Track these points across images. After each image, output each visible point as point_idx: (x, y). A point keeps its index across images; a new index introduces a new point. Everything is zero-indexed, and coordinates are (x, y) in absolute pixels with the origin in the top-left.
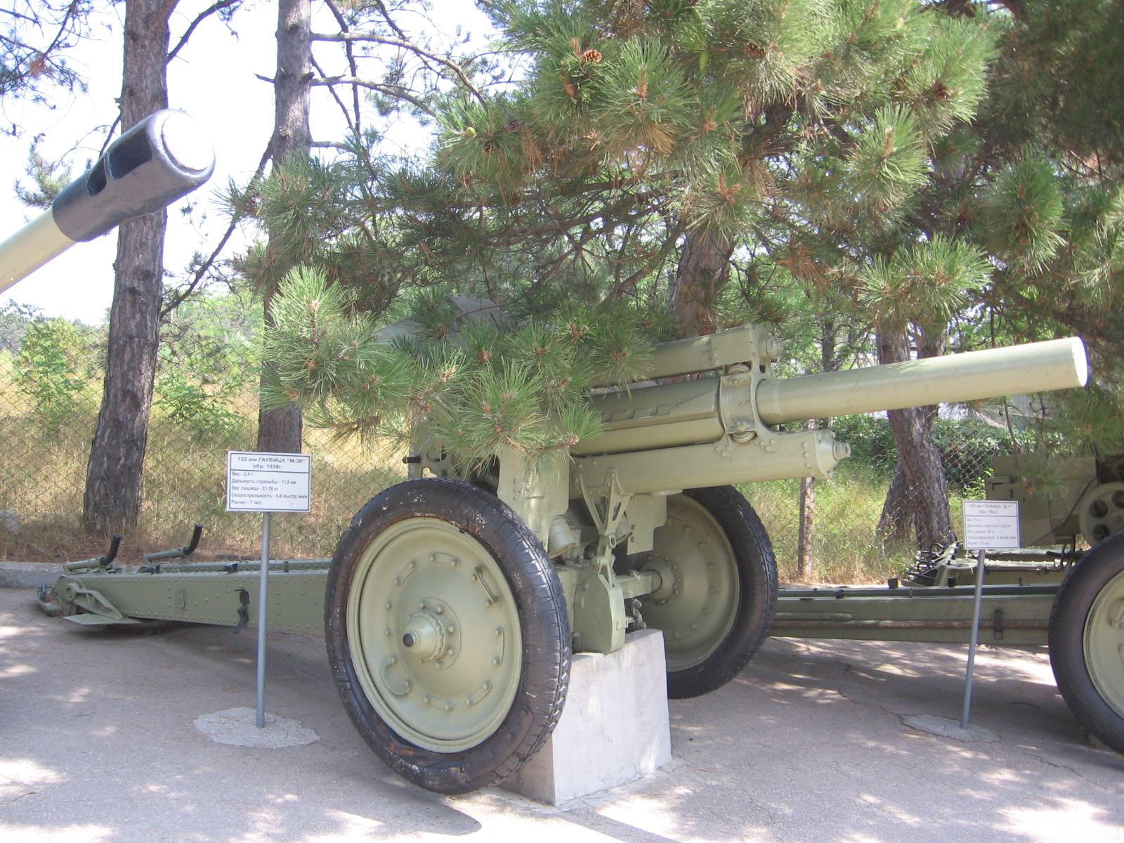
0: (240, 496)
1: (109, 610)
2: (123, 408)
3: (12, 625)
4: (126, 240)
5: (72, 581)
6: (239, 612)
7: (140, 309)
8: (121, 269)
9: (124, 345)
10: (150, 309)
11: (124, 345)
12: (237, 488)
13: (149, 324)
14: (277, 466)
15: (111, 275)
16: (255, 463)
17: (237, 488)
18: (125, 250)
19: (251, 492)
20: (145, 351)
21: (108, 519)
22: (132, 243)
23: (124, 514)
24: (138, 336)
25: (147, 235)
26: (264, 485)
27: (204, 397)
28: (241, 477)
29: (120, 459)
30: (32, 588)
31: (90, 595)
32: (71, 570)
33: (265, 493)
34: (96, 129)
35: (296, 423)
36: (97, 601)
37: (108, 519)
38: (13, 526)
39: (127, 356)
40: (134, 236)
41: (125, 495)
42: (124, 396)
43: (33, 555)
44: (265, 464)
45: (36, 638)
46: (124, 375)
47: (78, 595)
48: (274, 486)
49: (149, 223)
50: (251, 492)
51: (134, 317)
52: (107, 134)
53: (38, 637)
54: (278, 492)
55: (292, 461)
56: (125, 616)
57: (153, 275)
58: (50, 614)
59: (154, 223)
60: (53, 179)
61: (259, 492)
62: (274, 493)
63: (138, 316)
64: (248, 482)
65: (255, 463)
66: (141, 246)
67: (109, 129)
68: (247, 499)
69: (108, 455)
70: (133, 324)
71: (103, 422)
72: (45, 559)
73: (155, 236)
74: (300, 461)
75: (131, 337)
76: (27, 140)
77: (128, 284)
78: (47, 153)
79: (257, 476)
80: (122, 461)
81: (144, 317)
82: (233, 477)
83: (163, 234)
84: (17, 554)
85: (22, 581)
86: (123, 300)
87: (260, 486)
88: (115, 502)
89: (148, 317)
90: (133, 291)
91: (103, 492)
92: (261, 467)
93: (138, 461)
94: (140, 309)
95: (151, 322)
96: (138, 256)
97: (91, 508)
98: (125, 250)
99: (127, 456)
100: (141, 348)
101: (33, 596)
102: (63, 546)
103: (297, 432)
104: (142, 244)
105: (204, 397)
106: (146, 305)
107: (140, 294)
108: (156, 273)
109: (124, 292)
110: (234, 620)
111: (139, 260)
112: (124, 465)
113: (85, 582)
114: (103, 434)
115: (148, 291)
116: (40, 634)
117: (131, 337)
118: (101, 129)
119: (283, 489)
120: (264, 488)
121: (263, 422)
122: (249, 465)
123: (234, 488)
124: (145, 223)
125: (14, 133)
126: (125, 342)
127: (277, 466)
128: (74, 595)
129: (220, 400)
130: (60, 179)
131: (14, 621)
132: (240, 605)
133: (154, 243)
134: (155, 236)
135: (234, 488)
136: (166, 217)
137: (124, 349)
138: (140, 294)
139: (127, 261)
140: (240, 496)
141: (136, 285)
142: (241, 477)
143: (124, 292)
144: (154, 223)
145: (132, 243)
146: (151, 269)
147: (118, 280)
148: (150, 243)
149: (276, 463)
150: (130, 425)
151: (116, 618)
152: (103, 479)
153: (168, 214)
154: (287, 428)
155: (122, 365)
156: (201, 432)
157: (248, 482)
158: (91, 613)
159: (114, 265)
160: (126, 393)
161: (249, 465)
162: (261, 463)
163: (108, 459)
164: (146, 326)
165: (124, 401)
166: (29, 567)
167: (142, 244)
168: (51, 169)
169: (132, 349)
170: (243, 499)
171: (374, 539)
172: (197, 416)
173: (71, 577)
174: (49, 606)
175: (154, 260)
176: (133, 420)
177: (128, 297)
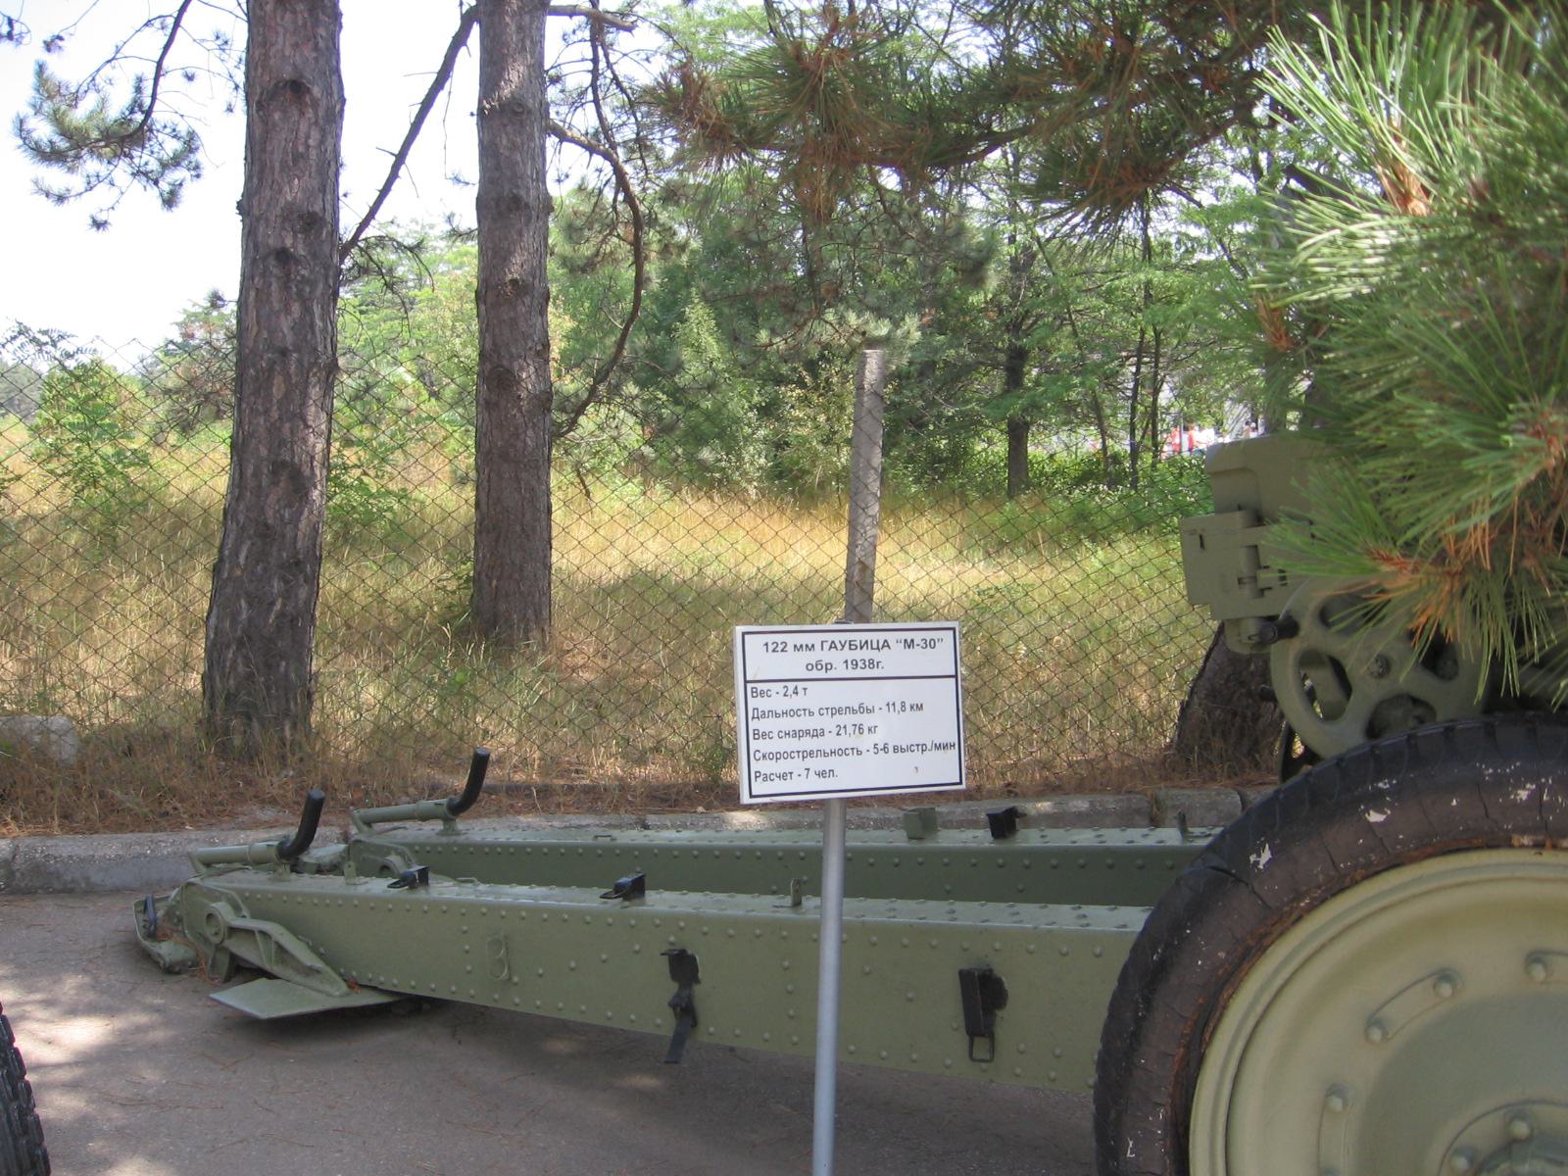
0: (777, 756)
1: (310, 971)
2: (272, 499)
3: (91, 1010)
4: (263, 150)
5: (215, 896)
6: (673, 1005)
7: (300, 293)
8: (255, 211)
9: (271, 370)
10: (319, 292)
11: (271, 370)
13: (319, 323)
14: (872, 664)
15: (235, 225)
16: (812, 657)
18: (262, 171)
19: (808, 744)
20: (314, 380)
21: (255, 724)
22: (277, 157)
23: (287, 713)
24: (298, 349)
25: (308, 137)
26: (840, 719)
27: (346, 468)
28: (776, 701)
29: (273, 603)
30: (116, 891)
31: (263, 933)
32: (208, 865)
33: (845, 741)
34: (148, 24)
35: (542, 506)
36: (281, 949)
37: (255, 724)
38: (67, 750)
39: (278, 390)
40: (279, 142)
41: (286, 675)
42: (274, 473)
43: (114, 818)
44: (836, 658)
45: (152, 1051)
46: (273, 429)
47: (233, 931)
48: (866, 720)
49: (310, 113)
50: (808, 744)
51: (287, 310)
52: (169, 31)
53: (155, 1046)
54: (879, 738)
55: (909, 644)
56: (354, 985)
57: (322, 219)
58: (170, 970)
59: (321, 113)
60: (79, 115)
61: (828, 742)
62: (866, 742)
63: (296, 308)
65: (812, 657)
66: (295, 161)
67: (170, 22)
68: (796, 765)
69: (248, 595)
70: (285, 324)
71: (232, 526)
72: (140, 823)
73: (322, 142)
74: (930, 644)
75: (284, 353)
76: (32, 51)
77: (271, 241)
78: (67, 69)
79: (819, 695)
80: (278, 606)
81: (307, 310)
83: (338, 137)
84: (80, 816)
85: (96, 878)
86: (263, 275)
87: (828, 723)
88: (268, 689)
89: (317, 310)
90: (283, 256)
91: (241, 668)
92: (828, 667)
93: (307, 602)
94: (300, 293)
95: (323, 320)
96: (290, 182)
97: (220, 703)
98: (262, 171)
99: (288, 594)
100: (305, 373)
101: (120, 918)
102: (173, 791)
103: (544, 523)
104: (298, 158)
105: (346, 468)
106: (313, 284)
107: (298, 262)
108: (328, 219)
109: (264, 259)
110: (663, 1023)
111: (293, 191)
112: (282, 615)
113: (245, 899)
114: (236, 553)
115: (314, 256)
116: (159, 1035)
117: (284, 353)
118: (157, 24)
119: (889, 727)
120: (840, 730)
121: (484, 506)
122: (793, 664)
123: (756, 732)
124: (302, 114)
125: (10, 36)
126: (272, 363)
127: (872, 664)
128: (223, 930)
129: (372, 473)
130: (90, 118)
131: (91, 996)
132: (673, 987)
133: (322, 153)
134: (322, 142)
136: (343, 101)
137: (270, 379)
138: (298, 262)
139: (268, 193)
140: (777, 756)
141: (289, 242)
142: (776, 701)
143: (264, 259)
144: (321, 113)
145: (277, 157)
146: (317, 208)
147: (250, 235)
148: (313, 153)
149: (866, 654)
150: (289, 531)
151: (332, 995)
152: (240, 643)
153: (347, 94)
154: (528, 516)
155: (266, 412)
156: (347, 526)
158: (270, 976)
159: (240, 206)
160: (278, 467)
161: (793, 664)
162: (828, 656)
163: (250, 605)
164: (312, 325)
165: (276, 483)
166: (109, 846)
167: (298, 158)
168: (75, 99)
169: (287, 377)
171: (1312, 908)
172: (337, 500)
173: (211, 883)
174: (167, 950)
175: (323, 190)
176: (295, 520)
177: (275, 269)
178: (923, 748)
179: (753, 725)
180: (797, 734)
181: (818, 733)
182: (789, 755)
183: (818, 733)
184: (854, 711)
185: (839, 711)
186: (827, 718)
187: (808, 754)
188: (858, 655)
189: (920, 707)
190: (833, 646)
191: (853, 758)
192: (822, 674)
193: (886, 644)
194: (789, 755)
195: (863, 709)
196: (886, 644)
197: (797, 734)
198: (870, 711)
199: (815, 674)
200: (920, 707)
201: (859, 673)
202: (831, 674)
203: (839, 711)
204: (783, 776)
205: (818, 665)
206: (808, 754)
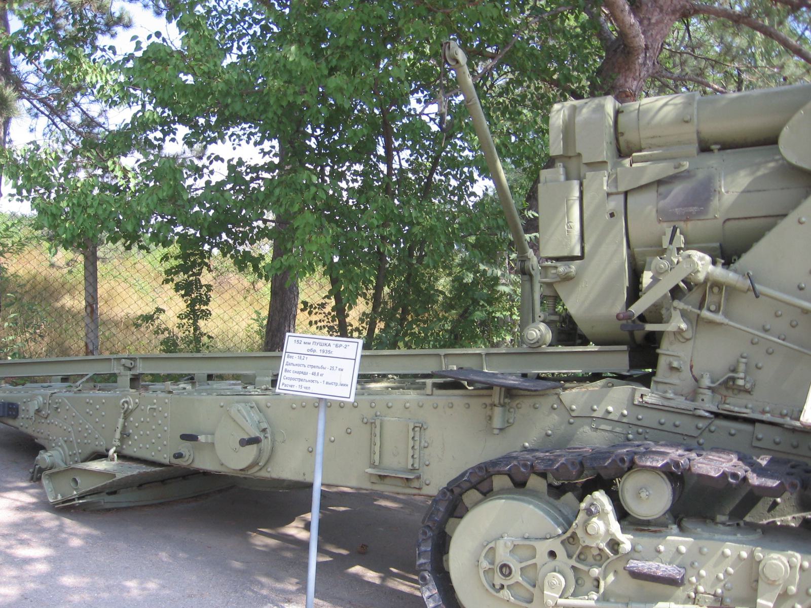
0: (291, 379)
12: (289, 371)
14: (330, 352)
16: (310, 347)
17: (289, 371)
19: (301, 376)
44: (318, 348)
50: (301, 376)
61: (310, 377)
65: (310, 347)
68: (296, 383)
87: (310, 371)
92: (314, 351)
119: (329, 376)
123: (286, 371)
135: (286, 371)
140: (291, 379)
142: (296, 360)
161: (303, 349)
170: (292, 382)
179: (285, 367)
180: (299, 373)
181: (305, 374)
182: (294, 379)
183: (305, 374)
184: (319, 368)
185: (314, 367)
186: (310, 368)
189: (342, 370)
191: (315, 384)
192: (312, 353)
194: (294, 379)
197: (299, 373)
198: (324, 368)
200: (342, 370)
201: (324, 354)
202: (315, 354)
203: (314, 367)
204: (291, 386)
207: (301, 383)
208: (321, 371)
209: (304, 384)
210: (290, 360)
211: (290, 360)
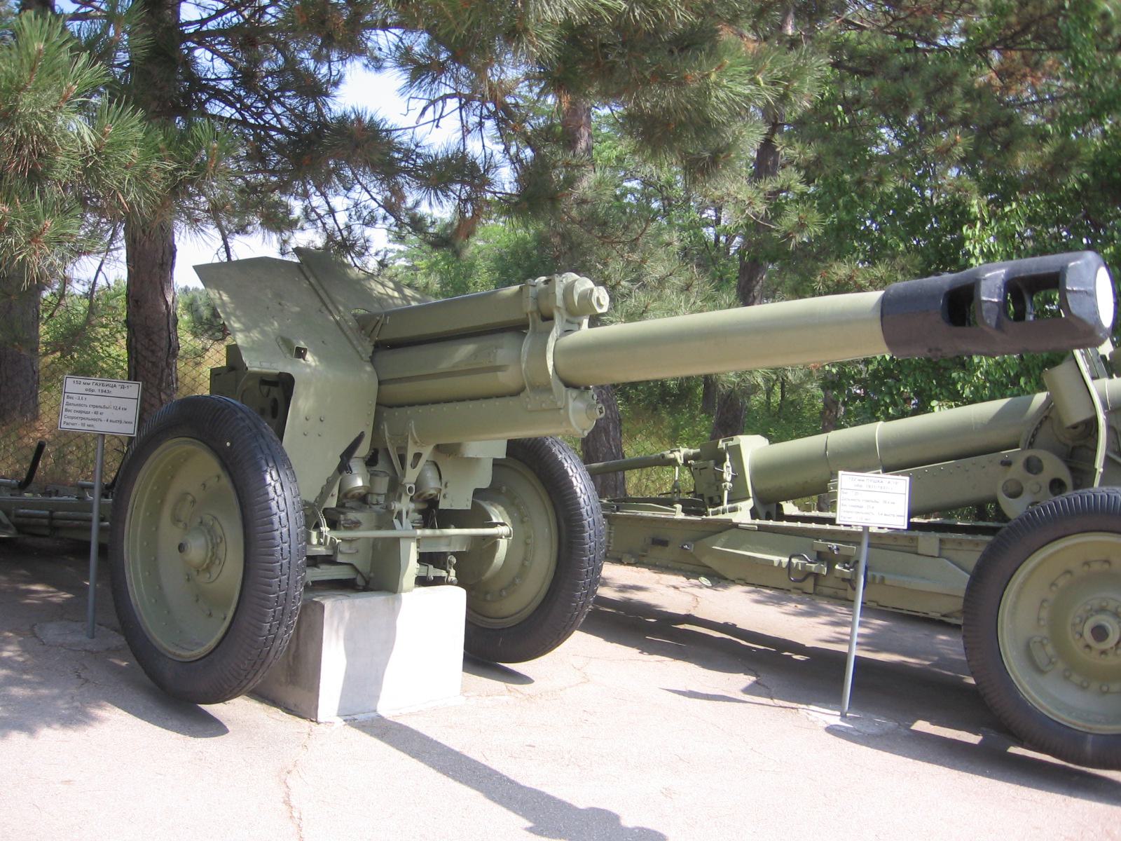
0: (72, 418)
12: (69, 411)
14: (109, 392)
16: (88, 387)
17: (69, 411)
19: (84, 415)
26: (96, 409)
28: (75, 401)
33: (96, 416)
44: (96, 388)
50: (84, 415)
64: (80, 405)
65: (88, 387)
68: (79, 422)
79: (92, 400)
82: (66, 400)
87: (92, 410)
122: (81, 388)
123: (66, 410)
135: (66, 410)
140: (72, 418)
157: (80, 405)
170: (74, 421)
178: (121, 422)
187: (83, 419)
188: (104, 388)
190: (97, 384)
193: (115, 386)
195: (104, 407)
196: (115, 386)
199: (87, 392)
202: (93, 393)
205: (90, 390)
206: (83, 419)
207: (83, 421)
208: (99, 410)
209: (88, 422)
210: (70, 401)
211: (70, 401)
